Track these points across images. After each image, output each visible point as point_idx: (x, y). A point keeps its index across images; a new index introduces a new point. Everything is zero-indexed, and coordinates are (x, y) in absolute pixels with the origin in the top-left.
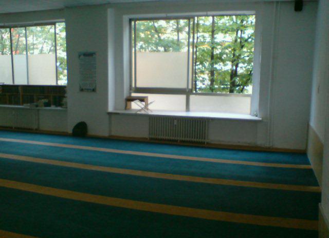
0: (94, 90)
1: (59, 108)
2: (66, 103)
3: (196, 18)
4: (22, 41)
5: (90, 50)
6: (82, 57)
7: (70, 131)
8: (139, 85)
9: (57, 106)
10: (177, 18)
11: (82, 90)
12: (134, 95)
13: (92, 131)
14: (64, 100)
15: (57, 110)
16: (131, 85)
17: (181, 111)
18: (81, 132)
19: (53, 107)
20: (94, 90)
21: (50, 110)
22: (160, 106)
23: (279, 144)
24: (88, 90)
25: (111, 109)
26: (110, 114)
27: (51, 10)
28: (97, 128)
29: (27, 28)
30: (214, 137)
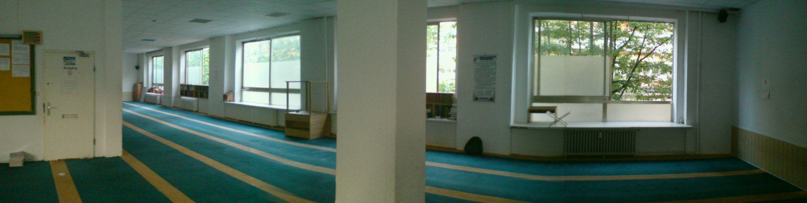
0: (492, 100)
1: (445, 120)
2: (455, 114)
3: (608, 23)
4: (599, 27)
5: (490, 53)
6: (478, 60)
7: (461, 147)
8: (543, 93)
9: (443, 116)
10: (591, 20)
11: (476, 99)
12: (535, 105)
13: (488, 149)
14: (452, 110)
15: (445, 122)
16: (532, 94)
17: (597, 121)
18: (474, 149)
19: (438, 119)
20: (492, 100)
21: (435, 122)
22: (574, 117)
23: (707, 149)
24: (484, 99)
25: (512, 124)
26: (513, 128)
27: (445, 7)
28: (495, 144)
29: (542, 21)
30: (642, 148)
